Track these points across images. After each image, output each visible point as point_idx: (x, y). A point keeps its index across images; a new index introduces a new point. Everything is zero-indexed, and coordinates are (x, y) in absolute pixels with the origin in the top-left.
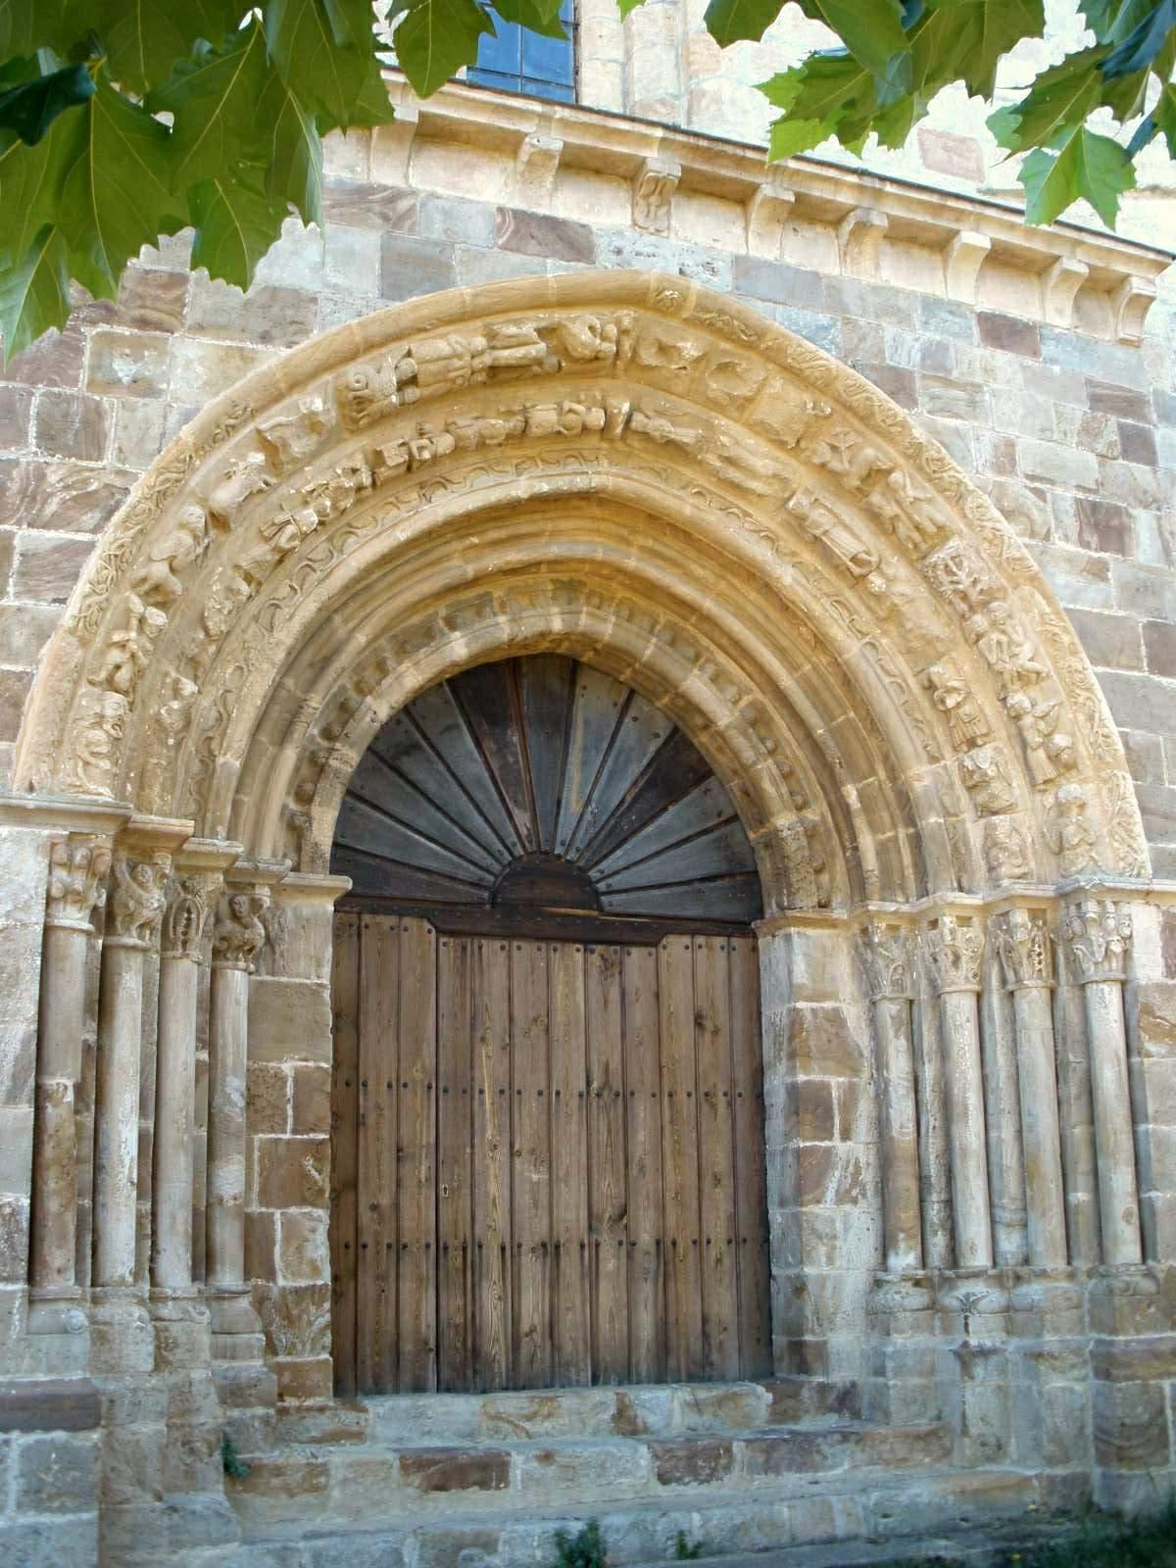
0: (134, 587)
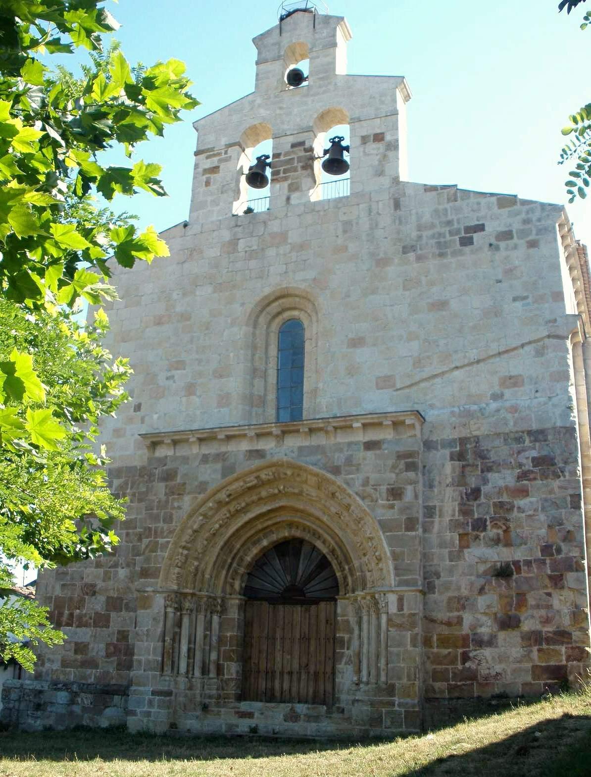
0: (180, 547)
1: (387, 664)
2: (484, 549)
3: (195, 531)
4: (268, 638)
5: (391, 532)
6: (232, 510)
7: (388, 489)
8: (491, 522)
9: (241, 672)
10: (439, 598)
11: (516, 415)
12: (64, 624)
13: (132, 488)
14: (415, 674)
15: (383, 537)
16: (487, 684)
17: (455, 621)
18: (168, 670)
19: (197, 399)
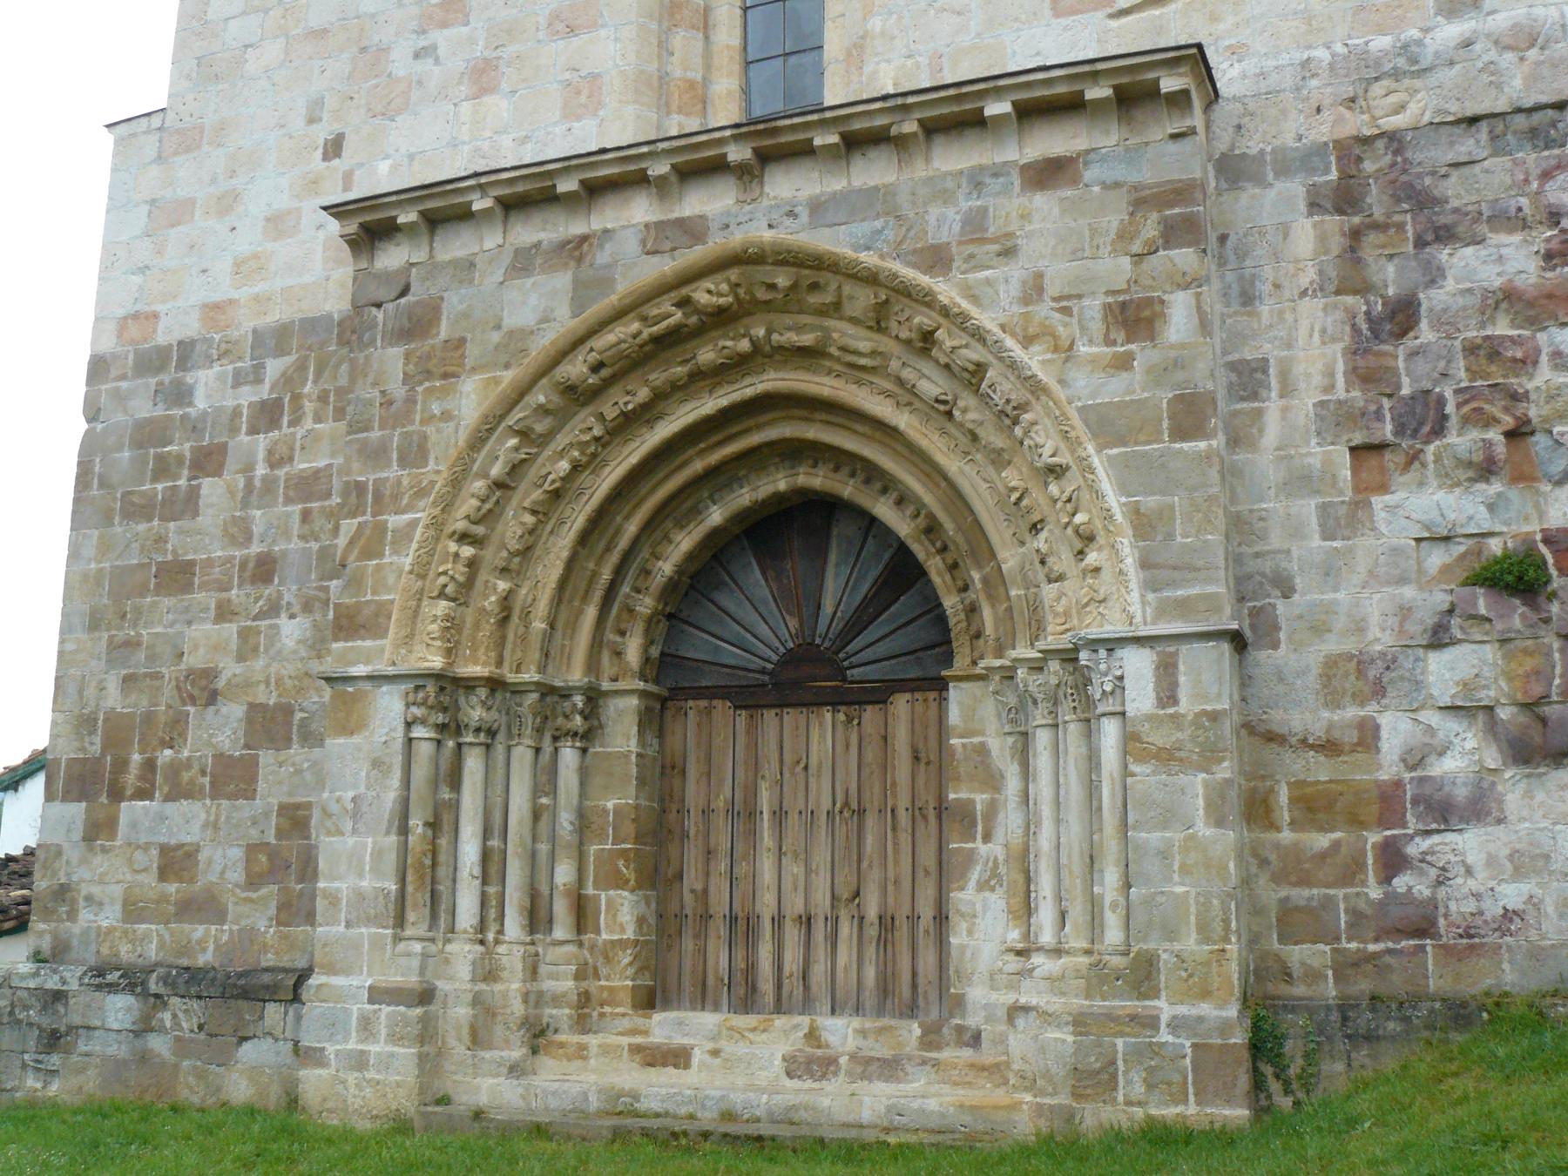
1: (1128, 886)
2: (1440, 495)
3: (499, 485)
4: (731, 810)
5: (1125, 444)
6: (611, 413)
7: (1108, 308)
8: (1459, 406)
9: (652, 920)
10: (1294, 660)
11: (1533, 54)
12: (129, 793)
13: (319, 373)
14: (1227, 921)
15: (1096, 462)
16: (1472, 947)
17: (1352, 736)
18: (416, 918)
19: (504, 104)
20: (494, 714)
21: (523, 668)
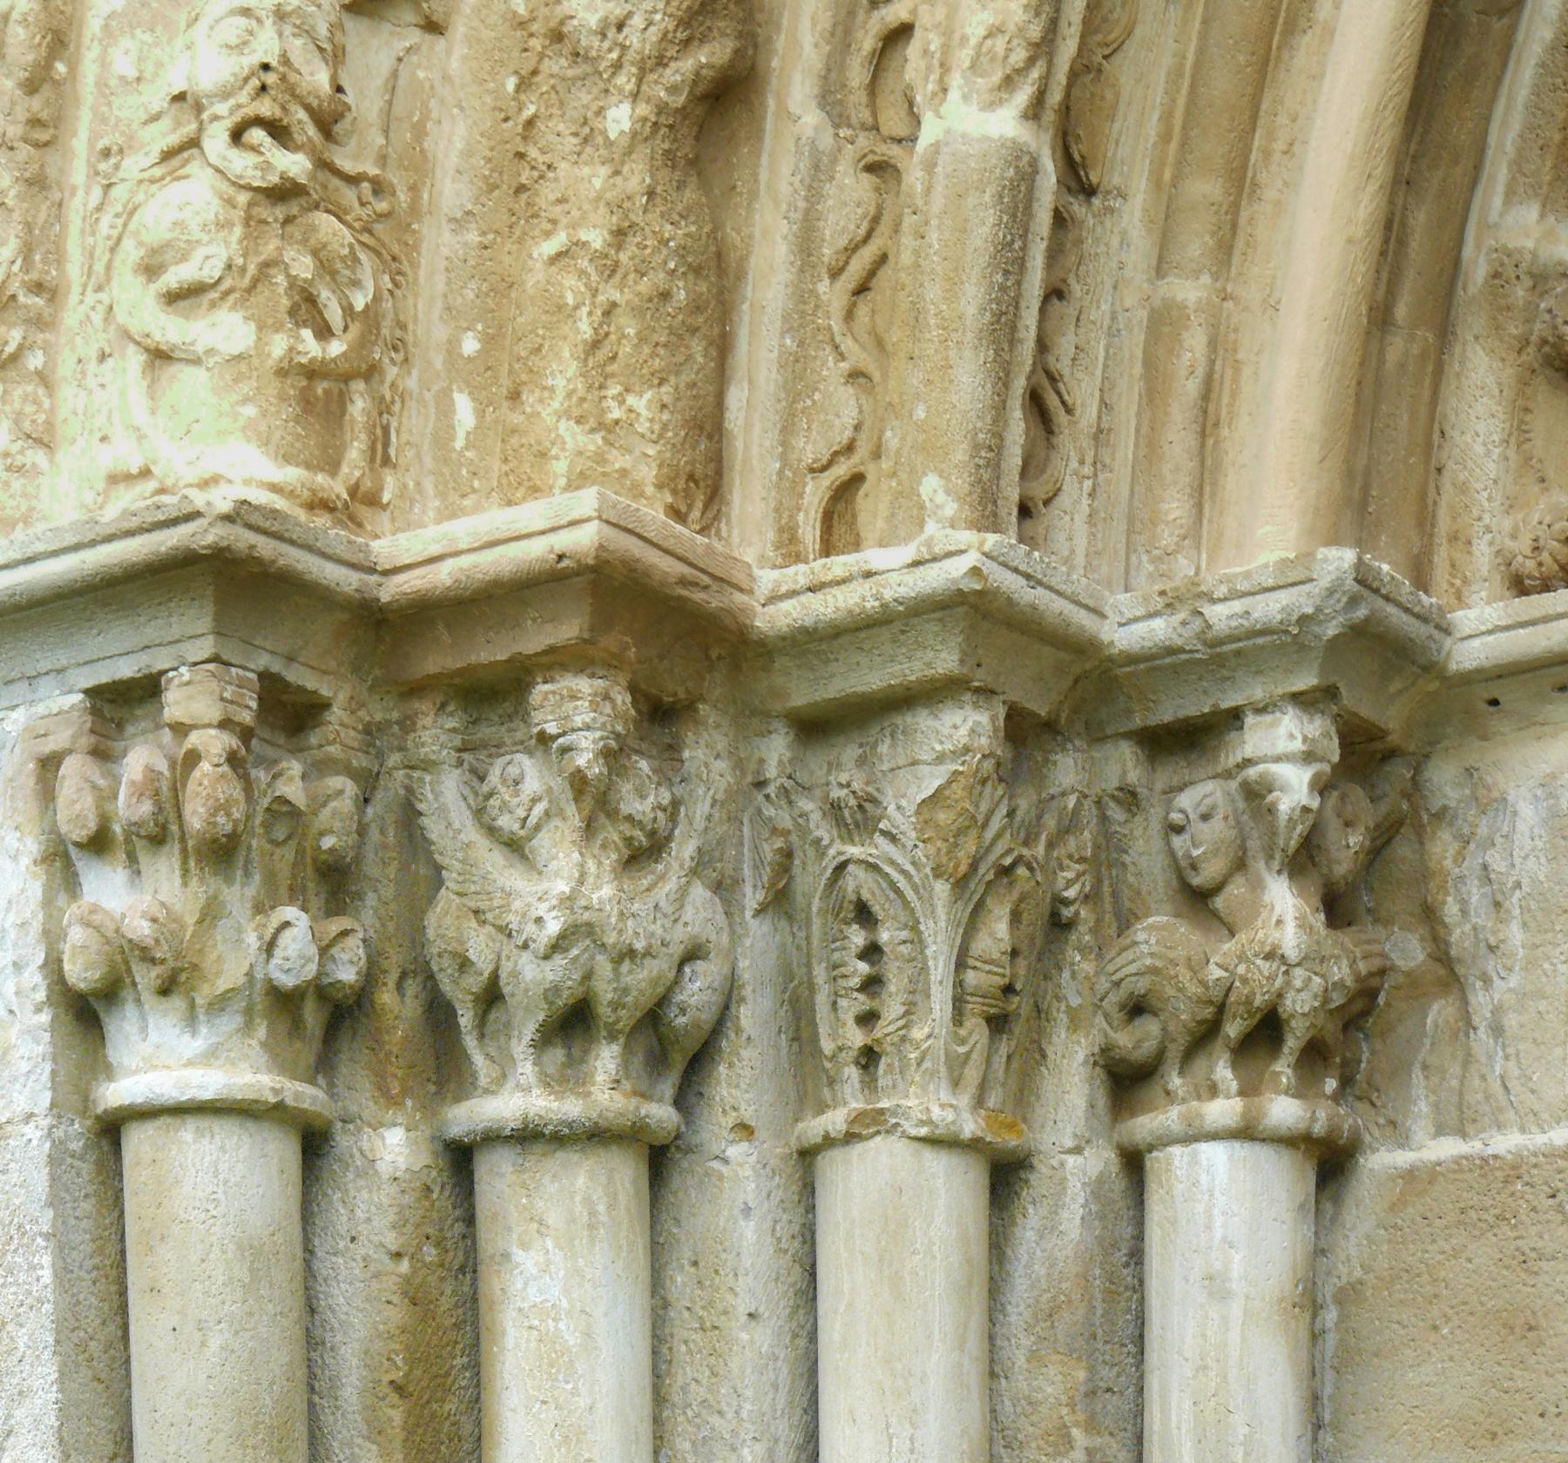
20: (667, 909)
21: (872, 507)
